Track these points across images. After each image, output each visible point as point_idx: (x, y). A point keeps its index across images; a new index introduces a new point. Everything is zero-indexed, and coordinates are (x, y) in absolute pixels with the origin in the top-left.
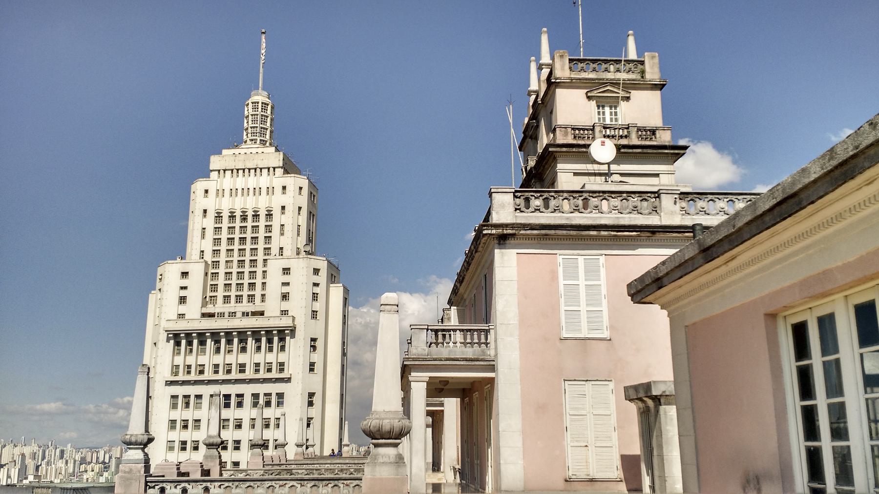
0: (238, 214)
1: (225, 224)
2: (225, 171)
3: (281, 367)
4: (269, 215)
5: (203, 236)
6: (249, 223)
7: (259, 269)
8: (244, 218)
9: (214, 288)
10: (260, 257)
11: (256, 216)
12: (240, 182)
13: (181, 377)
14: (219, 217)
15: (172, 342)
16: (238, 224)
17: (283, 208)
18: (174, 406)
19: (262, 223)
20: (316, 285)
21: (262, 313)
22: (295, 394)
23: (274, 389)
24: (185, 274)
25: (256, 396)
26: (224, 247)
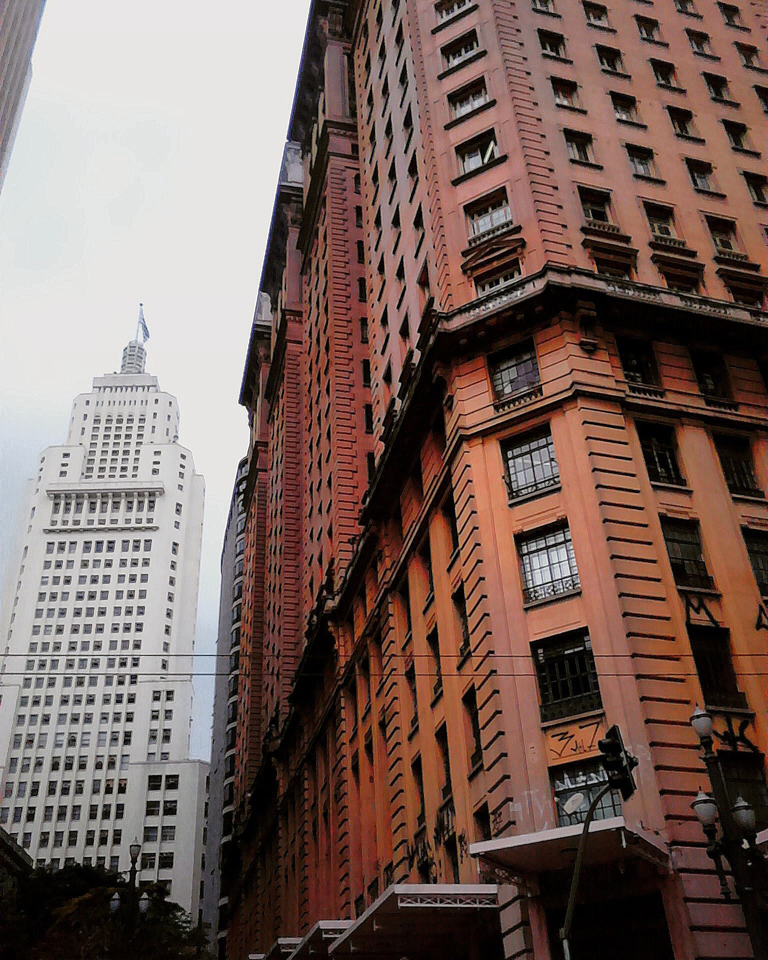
0: (115, 418)
1: (103, 425)
2: (105, 388)
3: (150, 521)
4: (142, 420)
5: (83, 433)
6: (124, 425)
7: (132, 456)
8: (120, 421)
9: (90, 469)
10: (132, 448)
11: (130, 420)
12: (118, 395)
13: (59, 526)
14: (97, 421)
15: (52, 502)
16: (114, 424)
17: (155, 414)
18: (49, 551)
19: (136, 424)
20: (182, 466)
22: (161, 542)
23: (142, 536)
24: (66, 455)
26: (100, 441)
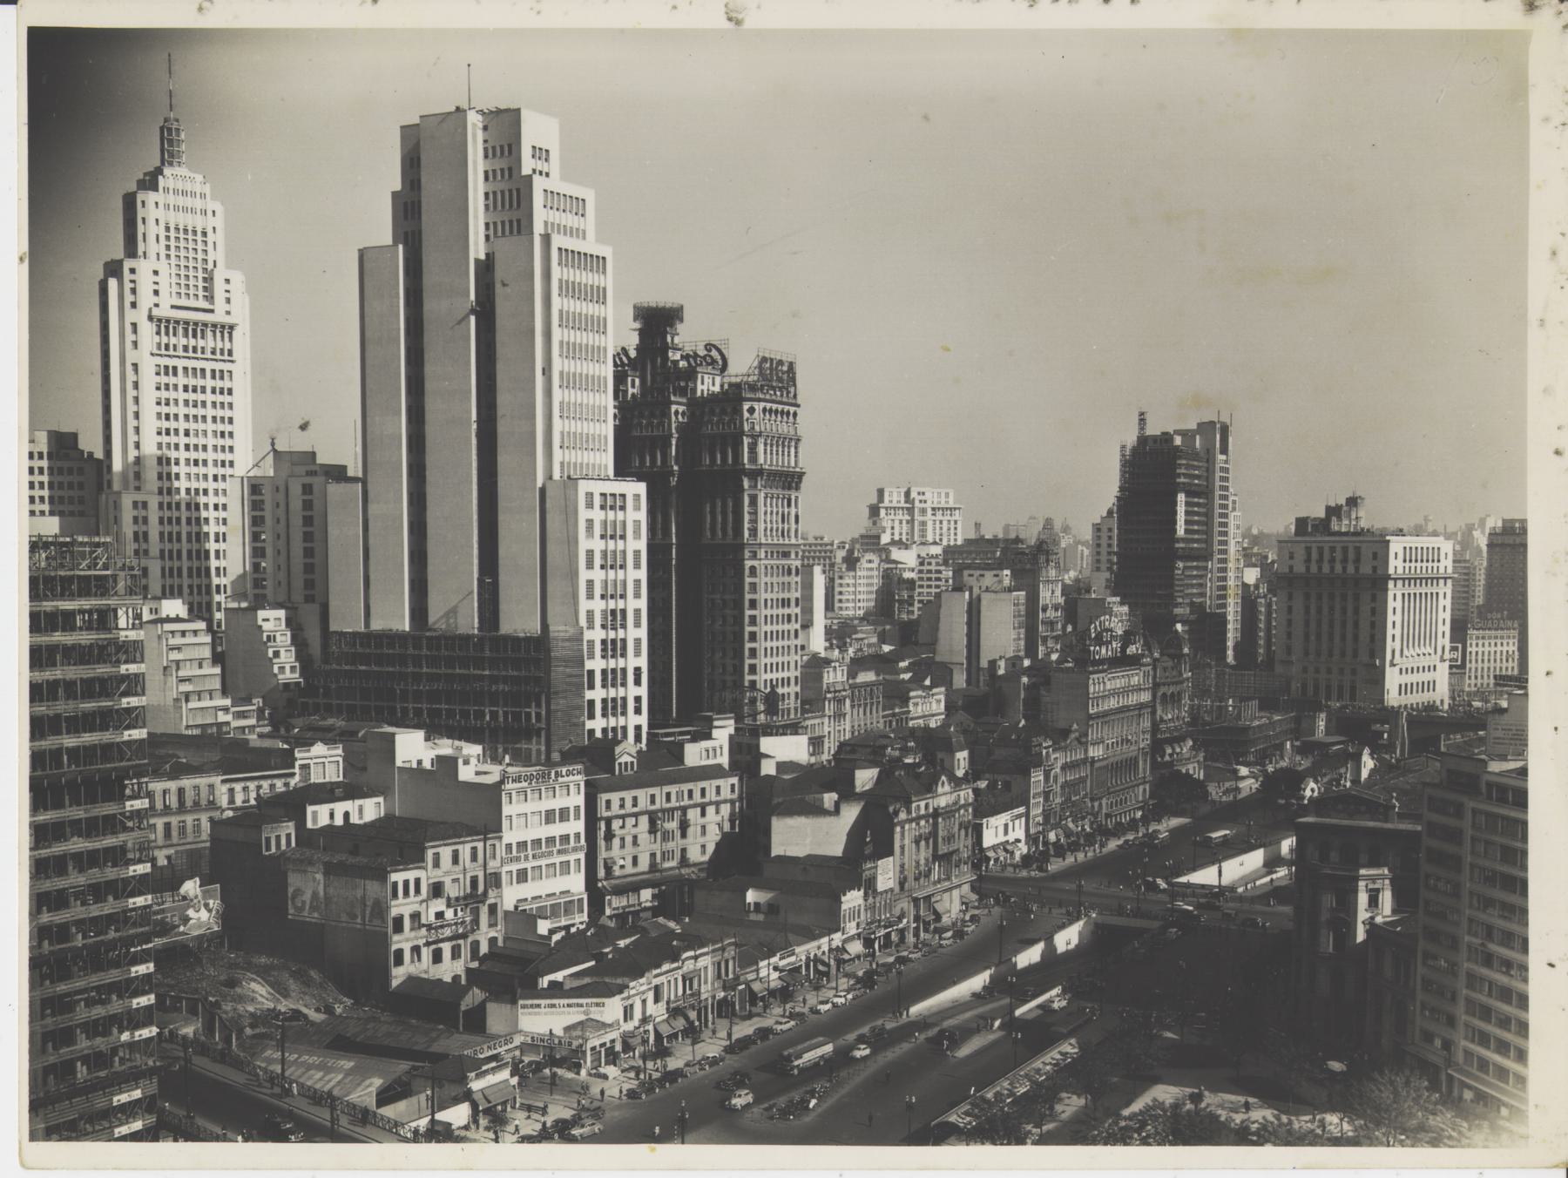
1: (172, 234)
3: (230, 353)
4: (204, 234)
11: (195, 232)
14: (168, 229)
21: (212, 311)
23: (226, 367)
24: (156, 273)
25: (213, 371)
